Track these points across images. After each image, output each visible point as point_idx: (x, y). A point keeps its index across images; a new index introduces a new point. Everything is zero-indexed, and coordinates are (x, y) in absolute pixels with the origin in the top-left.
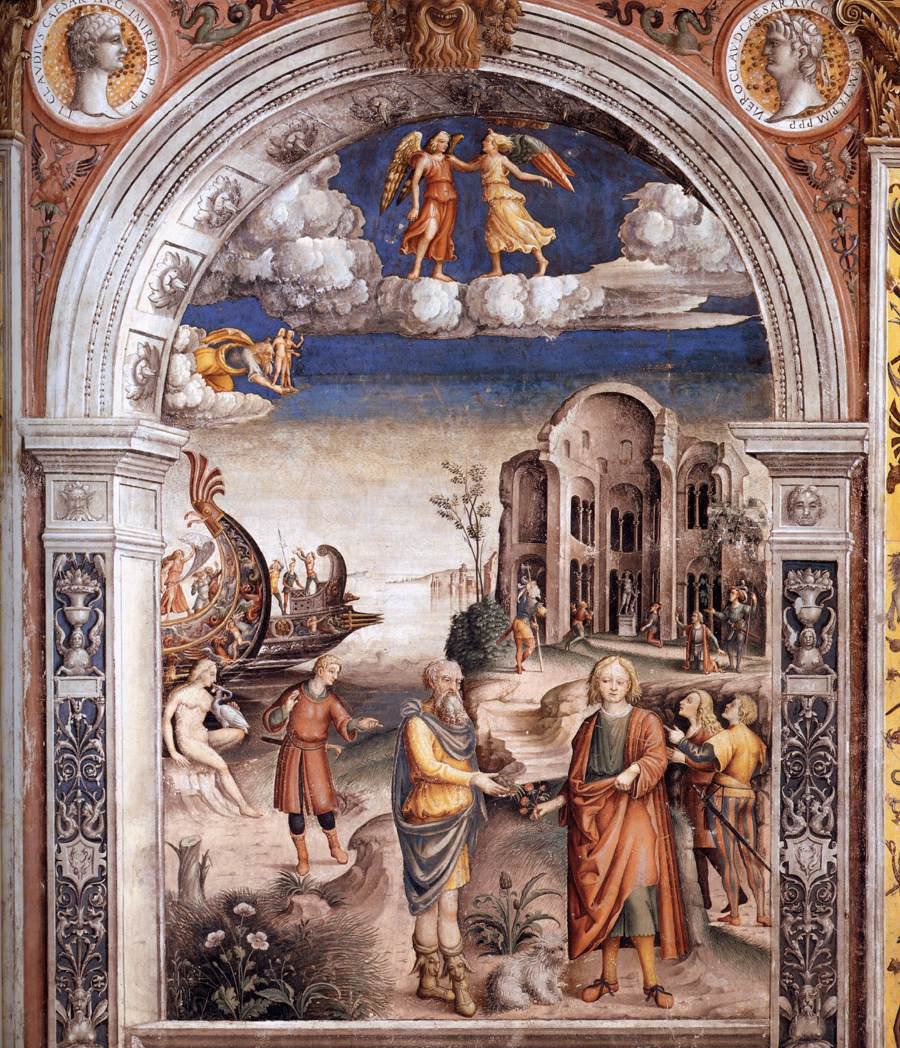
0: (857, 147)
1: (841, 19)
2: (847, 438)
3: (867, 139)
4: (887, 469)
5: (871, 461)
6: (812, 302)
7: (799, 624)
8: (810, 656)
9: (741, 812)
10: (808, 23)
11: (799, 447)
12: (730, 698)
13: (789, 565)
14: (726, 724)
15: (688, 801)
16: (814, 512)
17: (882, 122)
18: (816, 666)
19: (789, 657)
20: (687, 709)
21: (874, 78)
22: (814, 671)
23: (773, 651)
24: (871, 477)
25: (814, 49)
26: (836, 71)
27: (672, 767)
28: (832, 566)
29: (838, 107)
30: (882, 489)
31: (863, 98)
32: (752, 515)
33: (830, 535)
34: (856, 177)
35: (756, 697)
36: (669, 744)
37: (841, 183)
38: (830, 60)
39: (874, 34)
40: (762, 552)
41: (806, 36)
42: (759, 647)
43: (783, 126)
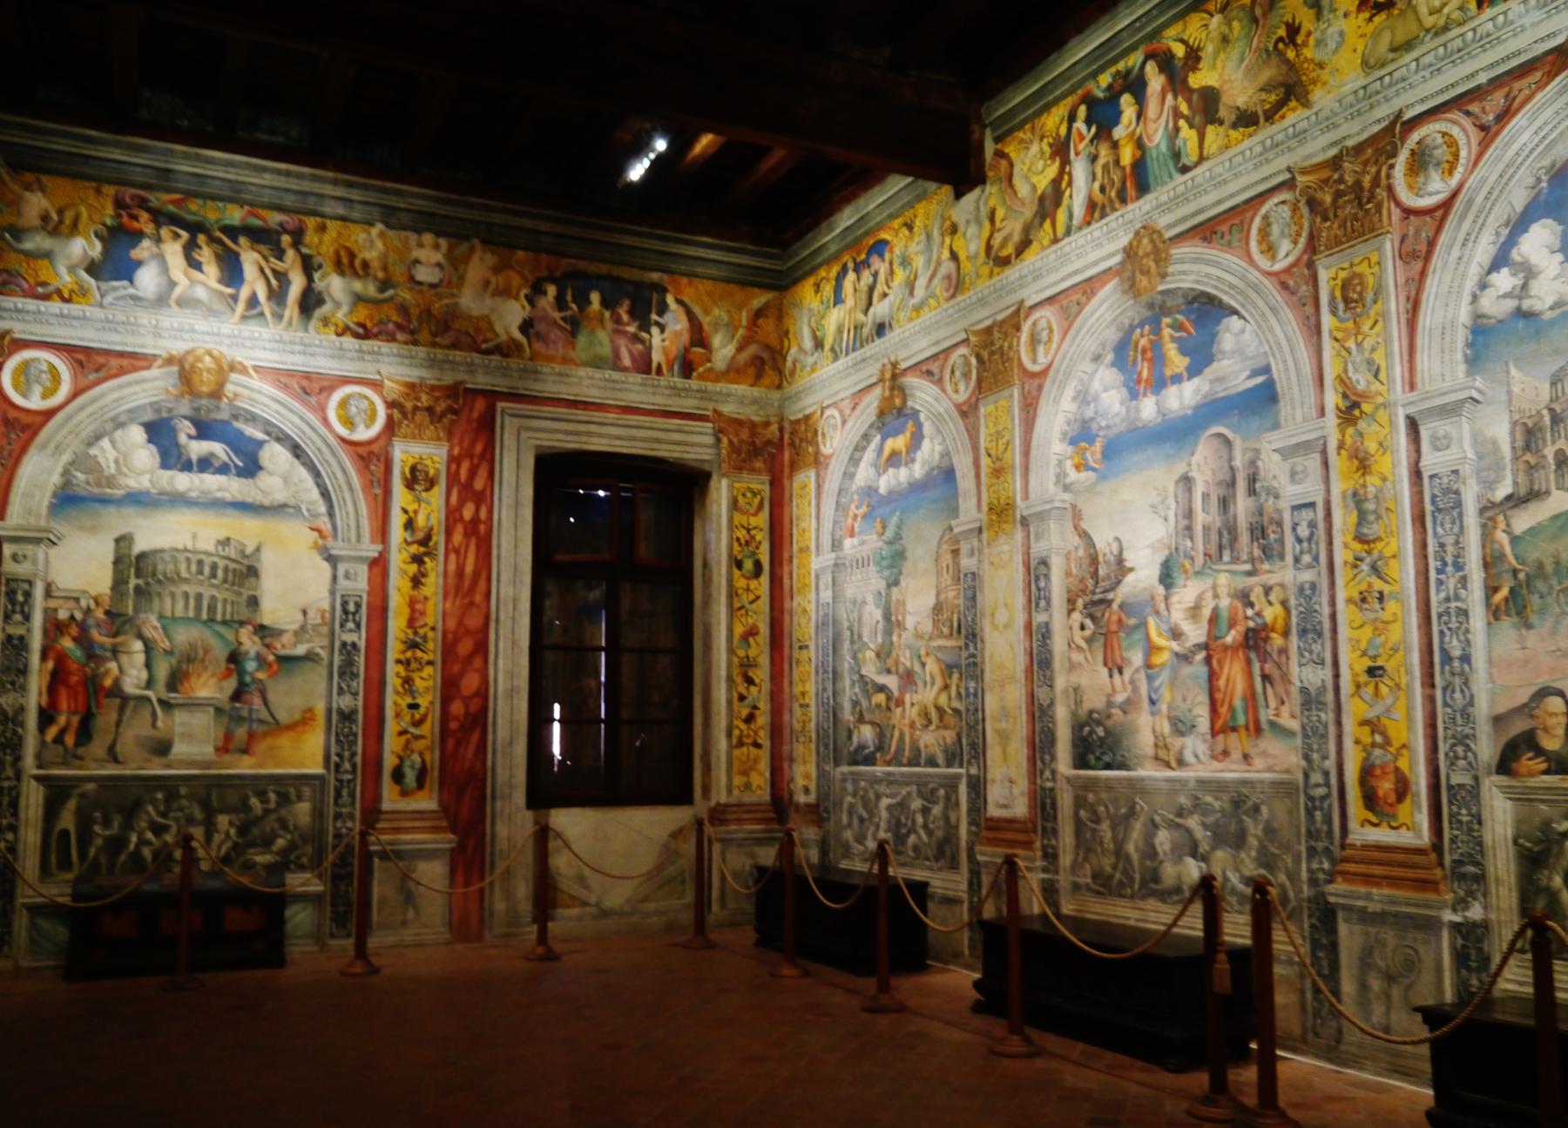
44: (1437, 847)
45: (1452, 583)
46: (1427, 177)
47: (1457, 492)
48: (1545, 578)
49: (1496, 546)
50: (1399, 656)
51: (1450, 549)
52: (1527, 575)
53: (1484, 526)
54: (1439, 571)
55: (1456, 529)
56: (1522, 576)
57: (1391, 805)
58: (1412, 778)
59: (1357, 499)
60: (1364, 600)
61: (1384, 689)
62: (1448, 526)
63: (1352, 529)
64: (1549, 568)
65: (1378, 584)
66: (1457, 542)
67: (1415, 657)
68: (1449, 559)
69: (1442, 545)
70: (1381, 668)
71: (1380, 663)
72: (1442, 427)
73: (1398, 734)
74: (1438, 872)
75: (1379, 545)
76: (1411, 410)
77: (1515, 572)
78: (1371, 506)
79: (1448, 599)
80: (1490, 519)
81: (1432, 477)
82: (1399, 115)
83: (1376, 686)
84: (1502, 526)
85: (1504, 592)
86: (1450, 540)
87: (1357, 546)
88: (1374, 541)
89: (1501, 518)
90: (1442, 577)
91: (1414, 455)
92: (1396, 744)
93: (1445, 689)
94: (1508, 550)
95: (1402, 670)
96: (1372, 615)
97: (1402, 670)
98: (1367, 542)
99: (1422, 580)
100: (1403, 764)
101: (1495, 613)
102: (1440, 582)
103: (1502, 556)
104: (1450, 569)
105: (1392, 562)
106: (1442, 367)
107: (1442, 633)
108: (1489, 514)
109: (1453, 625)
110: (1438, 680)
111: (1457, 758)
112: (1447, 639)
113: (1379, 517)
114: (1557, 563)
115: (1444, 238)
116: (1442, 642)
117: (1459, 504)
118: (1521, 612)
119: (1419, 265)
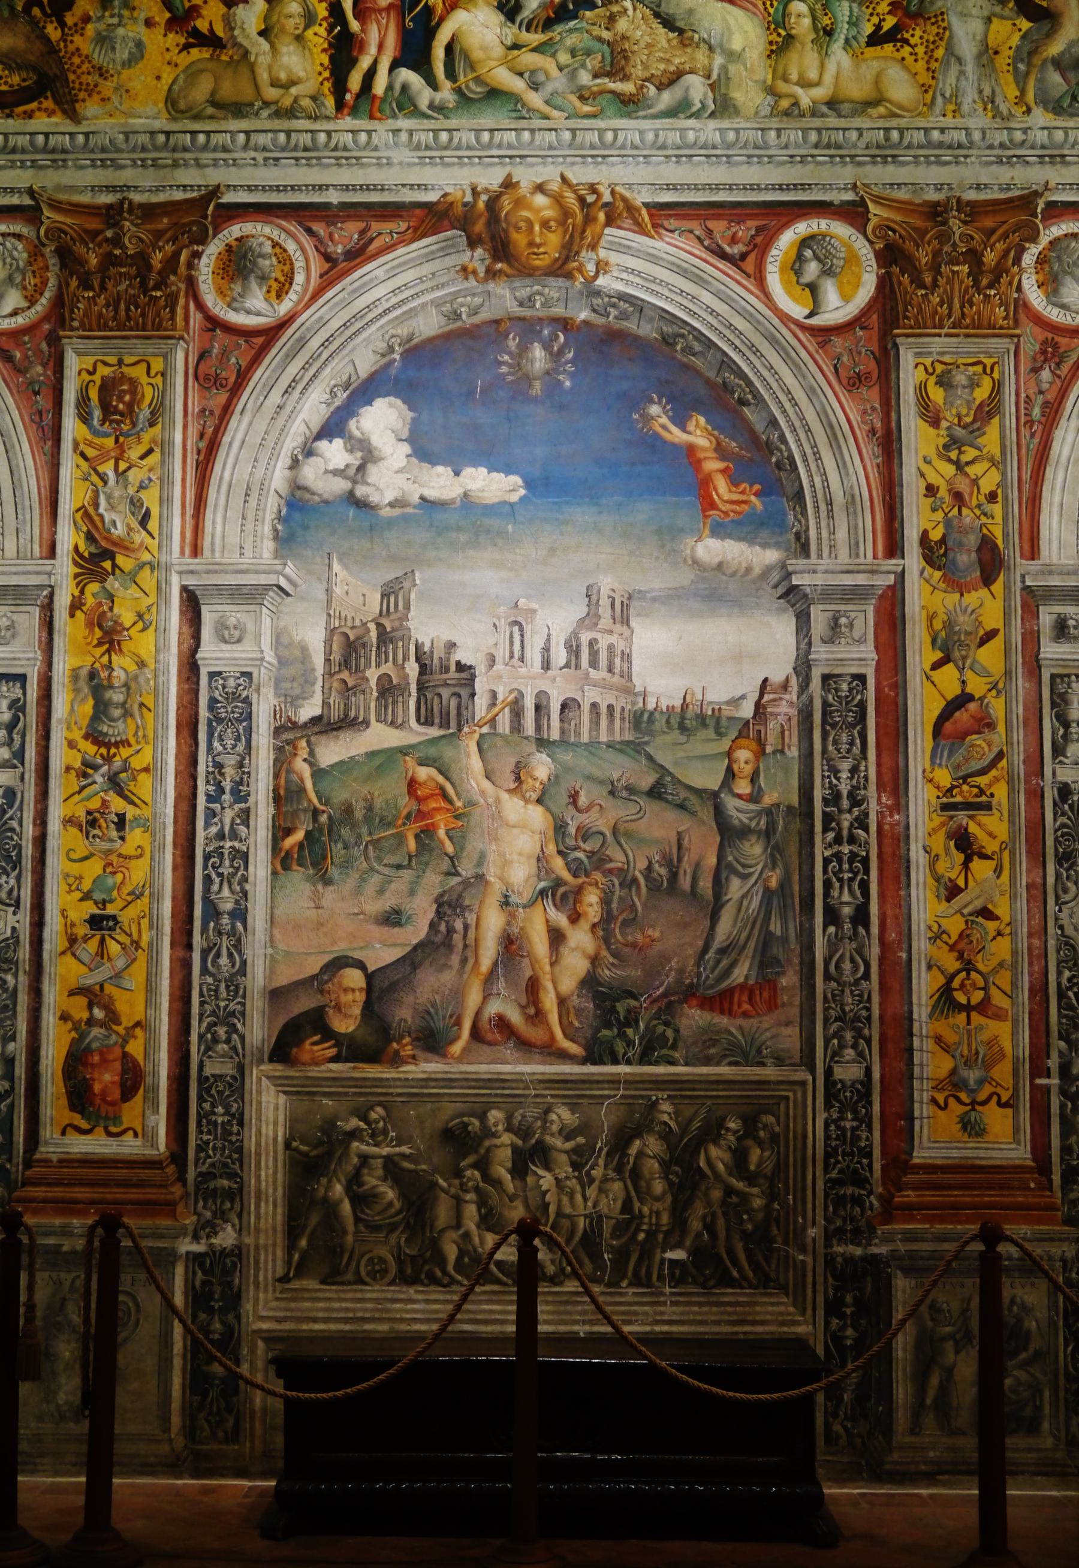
1: (44, 240)
2: (38, 573)
3: (61, 333)
4: (69, 599)
5: (57, 591)
6: (14, 463)
10: (17, 243)
16: (9, 634)
17: (73, 319)
18: (7, 761)
21: (68, 285)
24: (56, 606)
25: (21, 264)
26: (38, 280)
28: (22, 679)
29: (38, 308)
30: (65, 614)
31: (58, 302)
34: (51, 364)
37: (39, 369)
38: (34, 272)
39: (70, 251)
41: (15, 253)
44: (178, 1156)
45: (228, 816)
46: (245, 288)
47: (247, 701)
48: (354, 825)
49: (295, 778)
50: (142, 904)
51: (229, 771)
52: (330, 818)
53: (279, 750)
54: (210, 798)
55: (240, 748)
56: (323, 818)
57: (113, 1104)
59: (96, 684)
60: (93, 823)
61: (113, 947)
62: (229, 743)
63: (85, 723)
64: (359, 814)
65: (117, 804)
66: (241, 765)
67: (167, 907)
68: (227, 785)
69: (219, 766)
70: (114, 918)
71: (110, 910)
72: (236, 614)
73: (130, 1005)
74: (177, 1190)
75: (125, 752)
76: (190, 581)
77: (316, 813)
78: (117, 697)
79: (221, 836)
80: (288, 742)
81: (212, 675)
82: (215, 192)
83: (102, 941)
84: (304, 753)
85: (299, 836)
86: (230, 761)
87: (90, 748)
88: (117, 745)
89: (303, 743)
90: (216, 806)
91: (189, 642)
92: (126, 1022)
93: (205, 953)
94: (309, 784)
95: (145, 922)
96: (105, 846)
97: (145, 922)
98: (108, 745)
99: (185, 806)
100: (135, 1048)
101: (283, 861)
102: (211, 814)
103: (302, 790)
104: (227, 797)
105: (142, 777)
106: (240, 537)
107: (208, 880)
108: (288, 736)
109: (226, 870)
111: (216, 1040)
112: (215, 887)
113: (127, 714)
114: (370, 808)
115: (259, 374)
116: (207, 890)
117: (248, 717)
119: (223, 397)
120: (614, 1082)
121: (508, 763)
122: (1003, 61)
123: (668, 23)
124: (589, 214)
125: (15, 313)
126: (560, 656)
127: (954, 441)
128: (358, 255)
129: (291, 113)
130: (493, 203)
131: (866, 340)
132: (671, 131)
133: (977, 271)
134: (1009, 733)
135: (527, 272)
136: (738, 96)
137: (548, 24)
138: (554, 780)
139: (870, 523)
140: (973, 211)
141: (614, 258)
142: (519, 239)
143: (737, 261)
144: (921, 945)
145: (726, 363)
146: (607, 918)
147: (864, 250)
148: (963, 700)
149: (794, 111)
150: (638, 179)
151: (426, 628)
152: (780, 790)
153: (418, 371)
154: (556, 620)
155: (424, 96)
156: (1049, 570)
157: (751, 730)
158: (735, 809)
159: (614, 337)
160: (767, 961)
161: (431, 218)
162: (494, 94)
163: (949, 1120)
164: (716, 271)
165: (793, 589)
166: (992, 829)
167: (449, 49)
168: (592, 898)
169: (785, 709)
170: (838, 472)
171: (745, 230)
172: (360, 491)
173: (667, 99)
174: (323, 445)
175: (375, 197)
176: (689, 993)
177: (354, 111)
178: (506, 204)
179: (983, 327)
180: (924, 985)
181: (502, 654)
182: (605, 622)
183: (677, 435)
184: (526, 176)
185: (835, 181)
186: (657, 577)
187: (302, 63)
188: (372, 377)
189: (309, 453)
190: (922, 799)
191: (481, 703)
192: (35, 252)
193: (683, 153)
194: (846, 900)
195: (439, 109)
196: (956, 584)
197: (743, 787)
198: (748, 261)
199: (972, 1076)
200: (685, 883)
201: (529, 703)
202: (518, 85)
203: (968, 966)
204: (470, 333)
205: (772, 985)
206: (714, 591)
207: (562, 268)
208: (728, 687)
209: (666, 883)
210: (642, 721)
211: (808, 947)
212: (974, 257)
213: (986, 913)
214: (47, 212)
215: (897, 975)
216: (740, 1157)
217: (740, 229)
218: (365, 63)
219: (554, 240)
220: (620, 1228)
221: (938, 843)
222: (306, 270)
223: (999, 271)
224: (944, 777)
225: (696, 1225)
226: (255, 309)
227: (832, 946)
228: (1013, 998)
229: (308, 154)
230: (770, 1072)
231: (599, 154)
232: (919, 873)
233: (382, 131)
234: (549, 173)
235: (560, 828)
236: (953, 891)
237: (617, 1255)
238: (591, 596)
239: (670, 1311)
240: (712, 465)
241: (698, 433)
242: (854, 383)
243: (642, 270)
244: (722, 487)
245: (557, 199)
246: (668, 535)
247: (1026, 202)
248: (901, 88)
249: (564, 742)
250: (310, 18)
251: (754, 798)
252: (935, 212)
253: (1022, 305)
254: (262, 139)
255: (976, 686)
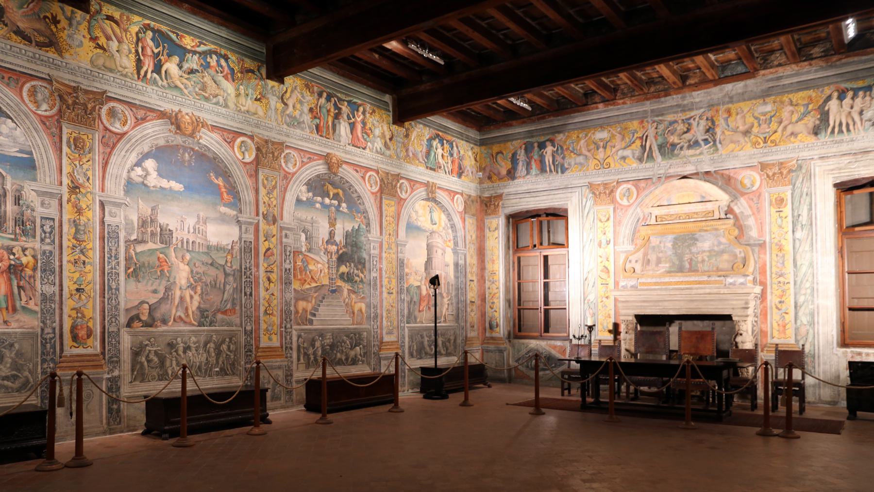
0: (59, 122)
7: (45, 233)
8: (48, 240)
9: (30, 277)
11: (44, 190)
12: (26, 249)
13: (42, 218)
14: (25, 255)
15: (15, 274)
19: (42, 240)
20: (14, 251)
22: (48, 244)
23: (38, 238)
27: (10, 265)
28: (53, 219)
31: (60, 111)
32: (32, 204)
33: (53, 212)
35: (33, 249)
36: (9, 259)
40: (35, 214)
42: (34, 237)
43: (39, 112)
44: (103, 353)
45: (114, 263)
58: (94, 330)
67: (98, 287)
72: (114, 210)
73: (88, 313)
74: (103, 362)
79: (112, 268)
82: (105, 92)
86: (114, 249)
93: (108, 299)
100: (90, 324)
106: (115, 189)
110: (106, 295)
118: (137, 276)
119: (109, 150)
120: (204, 331)
121: (180, 255)
122: (279, 112)
123: (215, 82)
124: (198, 124)
125: (46, 111)
126: (192, 230)
127: (268, 193)
128: (144, 119)
129: (125, 76)
130: (176, 115)
131: (253, 167)
132: (217, 108)
133: (273, 156)
134: (276, 257)
135: (184, 134)
136: (229, 104)
137: (189, 73)
138: (191, 260)
139: (253, 208)
140: (273, 143)
141: (203, 136)
142: (182, 126)
143: (229, 143)
144: (262, 301)
145: (226, 166)
146: (202, 293)
147: (254, 148)
148: (269, 249)
149: (240, 111)
150: (210, 118)
151: (162, 220)
152: (236, 266)
153: (160, 153)
154: (191, 222)
155: (160, 83)
156: (284, 223)
157: (230, 252)
158: (228, 270)
159: (203, 155)
160: (234, 304)
161: (162, 115)
162: (176, 87)
163: (266, 338)
164: (224, 144)
165: (238, 221)
166: (274, 277)
167: (166, 72)
168: (199, 288)
169: (237, 248)
170: (248, 196)
171: (231, 136)
172: (145, 182)
173: (215, 100)
174: (136, 168)
175: (147, 105)
176: (219, 311)
177: (142, 81)
178: (179, 116)
179: (274, 169)
180: (262, 309)
181: (179, 228)
182: (201, 223)
183: (216, 181)
184: (185, 110)
185: (248, 130)
186: (212, 214)
187: (128, 63)
188: (148, 153)
189: (133, 170)
190: (262, 269)
191: (174, 239)
192: (52, 94)
193: (218, 114)
194: (248, 291)
195: (164, 87)
196: (268, 224)
197: (229, 264)
198: (231, 143)
199: (270, 328)
200: (218, 285)
201: (185, 241)
202: (182, 86)
203: (270, 306)
204: (171, 147)
205: (234, 309)
206: (223, 219)
207: (192, 135)
208: (226, 242)
209: (214, 286)
210: (209, 247)
211: (241, 301)
212: (273, 153)
213: (273, 294)
214: (54, 83)
215: (257, 308)
216: (229, 347)
217: (231, 135)
218: (145, 69)
219: (190, 128)
220: (206, 364)
221: (265, 279)
222: (131, 121)
223: (277, 158)
224: (266, 265)
225: (220, 362)
226: (117, 128)
227: (246, 300)
228: (277, 313)
229: (130, 88)
230: (234, 328)
231: (200, 109)
232: (261, 286)
233: (149, 88)
234: (189, 111)
235: (192, 271)
236: (267, 290)
237: (206, 370)
238: (198, 216)
239: (216, 382)
240: (223, 190)
241: (220, 182)
242: (251, 176)
243: (210, 140)
244: (225, 194)
245: (191, 118)
246: (215, 205)
247: (282, 144)
248: (261, 113)
249: (192, 251)
250: (130, 52)
251: (231, 267)
252: (266, 142)
253: (281, 166)
254: (118, 81)
255: (271, 246)
